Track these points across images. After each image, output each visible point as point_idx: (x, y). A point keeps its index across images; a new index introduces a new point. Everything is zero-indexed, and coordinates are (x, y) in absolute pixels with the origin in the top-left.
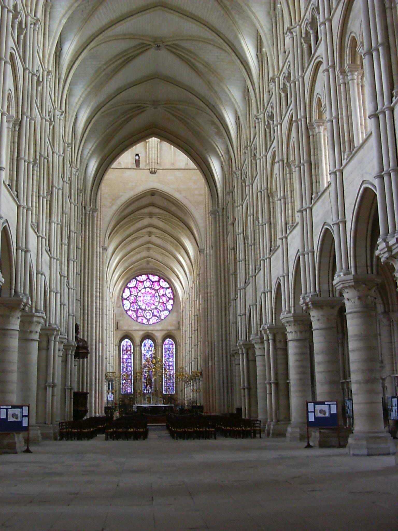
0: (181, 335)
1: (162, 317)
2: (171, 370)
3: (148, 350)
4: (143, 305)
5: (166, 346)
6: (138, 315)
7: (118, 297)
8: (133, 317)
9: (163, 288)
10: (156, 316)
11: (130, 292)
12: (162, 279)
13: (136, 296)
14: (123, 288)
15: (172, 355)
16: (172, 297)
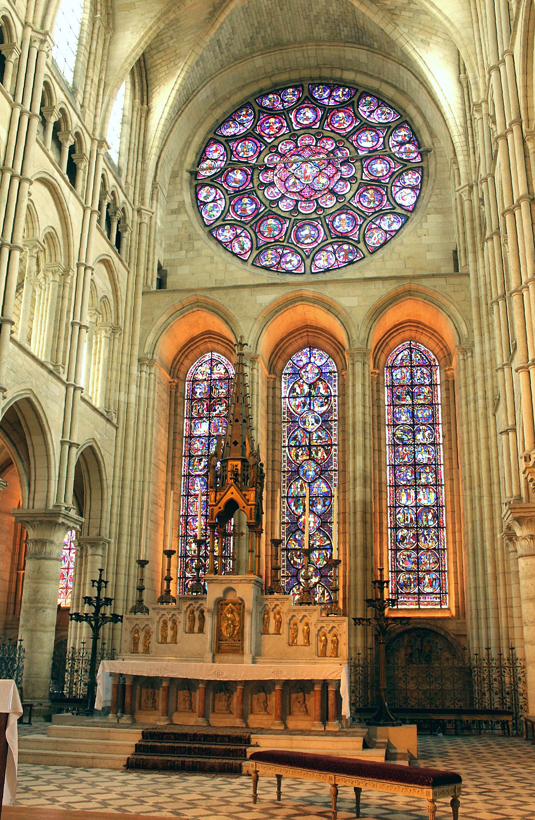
0: (467, 299)
1: (375, 239)
2: (426, 486)
3: (309, 395)
4: (283, 197)
5: (398, 374)
6: (262, 241)
7: (174, 175)
8: (237, 250)
9: (371, 127)
10: (344, 237)
11: (230, 152)
12: (371, 96)
13: (253, 168)
14: (198, 140)
15: (428, 412)
16: (418, 159)
